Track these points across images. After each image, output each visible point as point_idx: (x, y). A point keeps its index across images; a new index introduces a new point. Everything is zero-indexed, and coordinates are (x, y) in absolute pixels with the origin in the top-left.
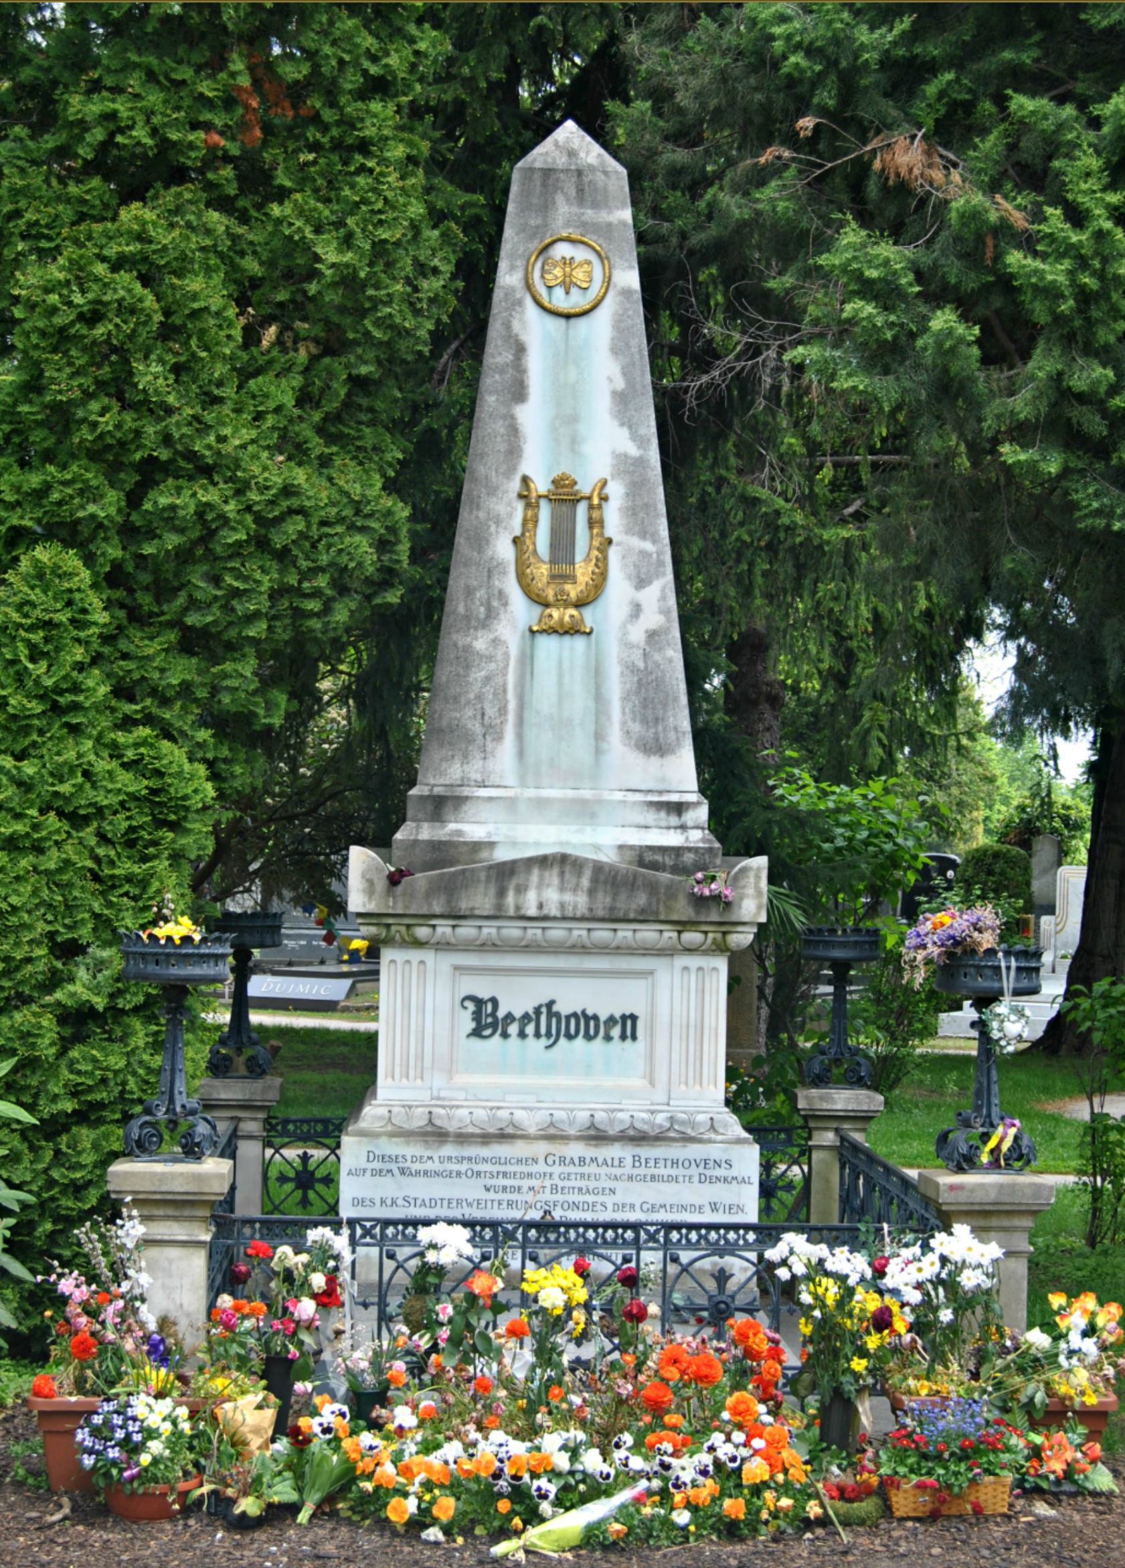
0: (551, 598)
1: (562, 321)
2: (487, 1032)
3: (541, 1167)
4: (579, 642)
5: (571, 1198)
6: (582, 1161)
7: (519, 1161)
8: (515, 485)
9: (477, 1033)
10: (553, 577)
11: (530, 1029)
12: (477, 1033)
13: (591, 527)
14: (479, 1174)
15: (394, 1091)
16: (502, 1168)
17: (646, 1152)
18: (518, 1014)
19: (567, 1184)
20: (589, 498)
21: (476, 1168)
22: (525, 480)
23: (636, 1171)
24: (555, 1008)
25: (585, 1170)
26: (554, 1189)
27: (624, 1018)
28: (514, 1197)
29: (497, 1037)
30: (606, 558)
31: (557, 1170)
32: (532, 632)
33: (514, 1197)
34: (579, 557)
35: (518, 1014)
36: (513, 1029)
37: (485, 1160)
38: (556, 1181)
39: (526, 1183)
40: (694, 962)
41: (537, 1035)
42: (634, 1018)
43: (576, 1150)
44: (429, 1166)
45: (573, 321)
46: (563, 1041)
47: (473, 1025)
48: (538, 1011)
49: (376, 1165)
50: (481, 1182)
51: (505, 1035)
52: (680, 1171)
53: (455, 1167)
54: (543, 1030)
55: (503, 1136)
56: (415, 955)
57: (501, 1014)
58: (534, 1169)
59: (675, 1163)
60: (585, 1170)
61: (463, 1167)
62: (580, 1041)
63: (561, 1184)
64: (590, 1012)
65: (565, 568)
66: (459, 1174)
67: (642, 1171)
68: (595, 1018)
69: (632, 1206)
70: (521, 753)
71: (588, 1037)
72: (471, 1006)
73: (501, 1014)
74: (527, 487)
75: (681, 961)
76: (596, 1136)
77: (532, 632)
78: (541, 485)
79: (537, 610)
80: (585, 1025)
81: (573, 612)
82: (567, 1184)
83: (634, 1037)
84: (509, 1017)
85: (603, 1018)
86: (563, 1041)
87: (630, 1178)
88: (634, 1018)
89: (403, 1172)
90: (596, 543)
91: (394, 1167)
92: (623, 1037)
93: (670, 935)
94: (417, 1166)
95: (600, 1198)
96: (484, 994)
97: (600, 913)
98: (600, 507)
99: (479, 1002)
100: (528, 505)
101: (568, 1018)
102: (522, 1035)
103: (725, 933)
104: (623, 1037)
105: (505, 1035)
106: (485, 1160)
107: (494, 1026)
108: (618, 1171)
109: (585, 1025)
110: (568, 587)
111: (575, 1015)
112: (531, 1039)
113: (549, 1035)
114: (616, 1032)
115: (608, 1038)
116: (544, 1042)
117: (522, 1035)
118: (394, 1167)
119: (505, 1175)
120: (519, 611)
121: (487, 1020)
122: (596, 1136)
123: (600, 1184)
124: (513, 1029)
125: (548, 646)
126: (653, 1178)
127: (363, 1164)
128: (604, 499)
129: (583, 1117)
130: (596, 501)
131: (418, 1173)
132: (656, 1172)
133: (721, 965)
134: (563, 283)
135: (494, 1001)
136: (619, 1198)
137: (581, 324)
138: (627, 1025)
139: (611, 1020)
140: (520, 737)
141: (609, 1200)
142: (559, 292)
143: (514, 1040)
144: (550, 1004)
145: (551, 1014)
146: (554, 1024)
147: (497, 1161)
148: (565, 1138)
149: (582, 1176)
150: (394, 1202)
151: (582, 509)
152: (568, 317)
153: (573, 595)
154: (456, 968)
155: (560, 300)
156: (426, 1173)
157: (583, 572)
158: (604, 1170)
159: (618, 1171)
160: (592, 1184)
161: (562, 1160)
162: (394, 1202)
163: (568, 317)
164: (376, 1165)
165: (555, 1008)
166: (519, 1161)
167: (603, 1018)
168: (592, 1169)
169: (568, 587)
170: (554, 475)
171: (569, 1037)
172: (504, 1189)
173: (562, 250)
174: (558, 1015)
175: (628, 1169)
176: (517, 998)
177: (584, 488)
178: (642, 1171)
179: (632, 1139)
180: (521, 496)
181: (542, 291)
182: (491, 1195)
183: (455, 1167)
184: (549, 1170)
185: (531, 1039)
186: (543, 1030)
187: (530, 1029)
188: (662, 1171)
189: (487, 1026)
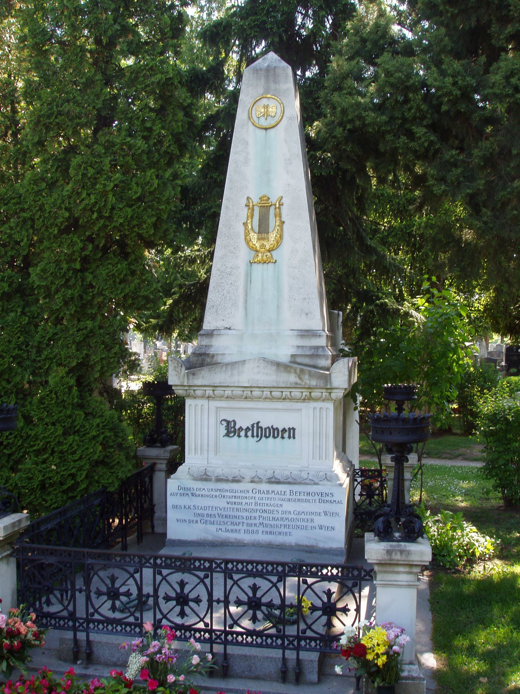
0: (258, 248)
1: (264, 131)
2: (232, 435)
3: (250, 494)
4: (271, 265)
5: (263, 508)
6: (268, 492)
7: (241, 491)
8: (245, 202)
9: (227, 435)
10: (259, 239)
11: (250, 433)
12: (227, 435)
13: (276, 217)
14: (224, 496)
15: (193, 460)
16: (234, 494)
17: (296, 488)
18: (244, 428)
19: (261, 502)
20: (275, 205)
21: (223, 494)
22: (248, 198)
23: (291, 497)
24: (260, 425)
25: (270, 496)
26: (256, 504)
27: (289, 429)
28: (239, 507)
29: (236, 437)
30: (282, 229)
31: (257, 496)
32: (251, 263)
33: (239, 507)
34: (271, 230)
35: (244, 428)
36: (243, 433)
37: (227, 491)
38: (257, 500)
39: (244, 501)
40: (319, 405)
41: (253, 436)
42: (294, 429)
43: (265, 487)
44: (203, 492)
45: (268, 130)
46: (263, 438)
47: (226, 431)
48: (253, 426)
49: (182, 491)
50: (225, 500)
51: (239, 436)
52: (311, 498)
53: (214, 493)
54: (255, 434)
55: (236, 480)
56: (199, 402)
57: (237, 427)
58: (247, 495)
59: (308, 494)
60: (270, 496)
61: (218, 493)
62: (271, 439)
63: (259, 502)
64: (275, 427)
65: (264, 235)
66: (216, 496)
67: (294, 497)
68: (277, 429)
69: (290, 512)
70: (246, 315)
71: (274, 437)
72: (225, 424)
73: (237, 427)
74: (249, 203)
75: (313, 404)
76: (273, 481)
77: (251, 263)
78: (255, 200)
79: (253, 253)
80: (274, 432)
81: (268, 254)
82: (261, 502)
83: (294, 438)
84: (241, 429)
85: (280, 430)
86: (263, 438)
87: (289, 500)
88: (294, 429)
89: (193, 495)
90: (277, 224)
91: (189, 492)
92: (289, 437)
93: (306, 393)
94: (198, 493)
95: (276, 508)
96: (230, 419)
97: (275, 385)
98: (279, 208)
99: (228, 422)
100: (249, 209)
101: (265, 429)
102: (246, 436)
103: (330, 393)
104: (289, 437)
105: (239, 436)
106: (227, 491)
107: (235, 432)
108: (284, 497)
109: (274, 432)
110: (265, 243)
111: (268, 427)
112: (250, 438)
113: (257, 436)
114: (286, 435)
115: (283, 437)
116: (256, 439)
117: (246, 436)
118: (189, 492)
119: (235, 497)
120: (244, 254)
121: (231, 429)
122: (273, 481)
123: (277, 502)
124: (243, 433)
125: (258, 269)
126: (299, 500)
127: (176, 490)
128: (281, 205)
129: (269, 474)
130: (277, 206)
131: (199, 495)
132: (300, 497)
133: (330, 406)
134: (264, 115)
135: (234, 421)
136: (284, 508)
137: (272, 132)
138: (291, 432)
139: (284, 430)
140: (246, 308)
141: (280, 509)
142: (262, 119)
143: (243, 438)
144: (258, 422)
145: (258, 427)
146: (260, 432)
147: (232, 491)
148: (260, 481)
149: (268, 499)
150: (189, 507)
151: (272, 209)
152: (266, 129)
153: (268, 247)
154: (217, 408)
155: (263, 122)
156: (202, 495)
157: (273, 236)
158: (277, 496)
159: (284, 497)
160: (272, 502)
161: (259, 491)
162: (189, 507)
163: (266, 129)
164: (182, 491)
165: (260, 425)
166: (241, 491)
167: (280, 430)
168: (273, 496)
169: (265, 243)
170: (261, 195)
171: (266, 437)
172: (235, 503)
173: (265, 102)
174: (261, 428)
175: (288, 496)
176: (243, 421)
177: (274, 200)
178: (294, 497)
179: (289, 483)
180: (246, 206)
181: (256, 120)
182: (230, 506)
183: (214, 493)
184: (254, 495)
185: (250, 438)
186: (255, 434)
187: (250, 433)
188: (302, 497)
189: (231, 432)
